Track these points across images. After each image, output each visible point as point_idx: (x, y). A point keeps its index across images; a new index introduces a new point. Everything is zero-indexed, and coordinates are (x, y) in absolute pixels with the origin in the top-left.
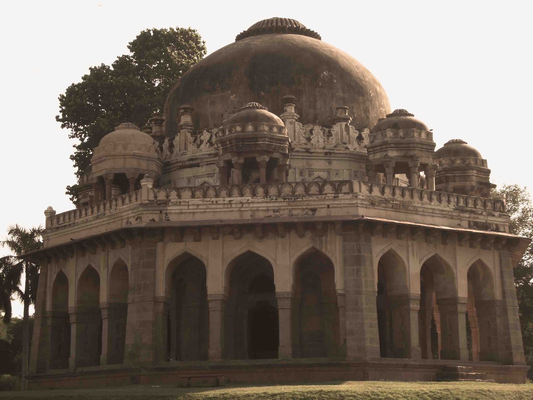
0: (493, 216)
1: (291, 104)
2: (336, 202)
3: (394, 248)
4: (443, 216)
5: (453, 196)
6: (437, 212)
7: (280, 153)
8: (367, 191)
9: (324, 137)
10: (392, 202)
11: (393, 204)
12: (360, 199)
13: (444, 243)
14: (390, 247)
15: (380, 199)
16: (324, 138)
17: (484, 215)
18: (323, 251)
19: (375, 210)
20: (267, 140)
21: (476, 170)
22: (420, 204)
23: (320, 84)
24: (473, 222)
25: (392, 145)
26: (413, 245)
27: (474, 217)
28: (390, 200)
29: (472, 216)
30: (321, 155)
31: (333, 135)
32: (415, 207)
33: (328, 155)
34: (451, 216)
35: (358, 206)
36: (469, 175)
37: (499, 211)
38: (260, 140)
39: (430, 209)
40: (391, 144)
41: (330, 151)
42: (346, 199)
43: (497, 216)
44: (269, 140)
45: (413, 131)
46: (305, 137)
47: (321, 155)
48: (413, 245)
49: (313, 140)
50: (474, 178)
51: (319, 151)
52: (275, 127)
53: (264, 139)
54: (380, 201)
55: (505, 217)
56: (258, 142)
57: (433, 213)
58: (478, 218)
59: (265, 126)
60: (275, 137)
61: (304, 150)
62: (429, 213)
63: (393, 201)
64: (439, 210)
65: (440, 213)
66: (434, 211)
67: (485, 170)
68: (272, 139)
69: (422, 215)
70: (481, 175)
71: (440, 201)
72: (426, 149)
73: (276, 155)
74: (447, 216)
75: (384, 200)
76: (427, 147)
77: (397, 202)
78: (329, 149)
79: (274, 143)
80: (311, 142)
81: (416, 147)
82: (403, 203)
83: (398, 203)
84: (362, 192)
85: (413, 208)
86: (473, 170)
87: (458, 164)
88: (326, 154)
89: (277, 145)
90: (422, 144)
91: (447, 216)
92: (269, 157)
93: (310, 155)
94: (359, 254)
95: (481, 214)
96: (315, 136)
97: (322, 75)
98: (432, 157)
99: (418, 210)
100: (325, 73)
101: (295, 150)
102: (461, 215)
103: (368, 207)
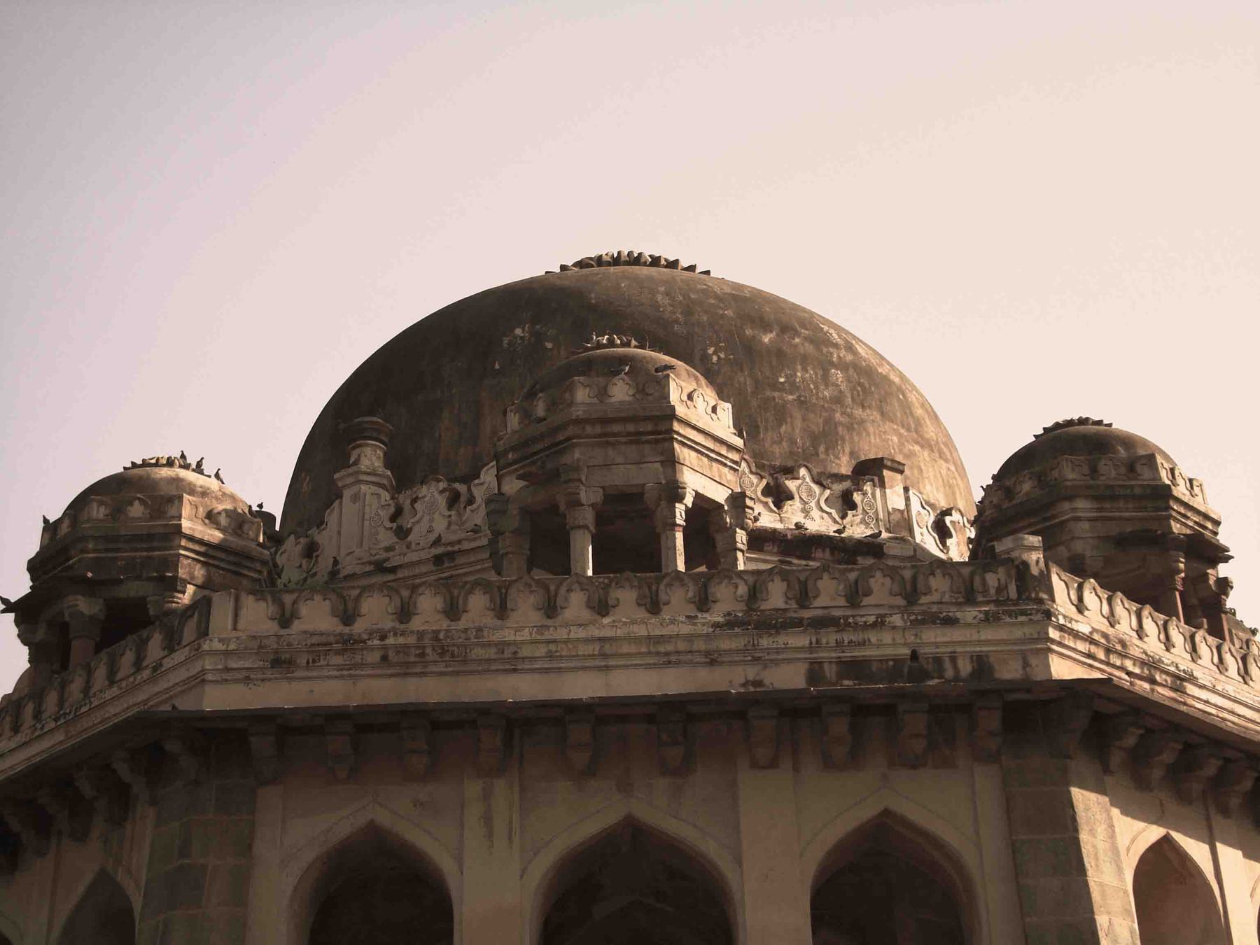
0: (950, 622)
1: (358, 442)
2: (163, 685)
3: (383, 818)
4: (666, 659)
5: (731, 578)
6: (625, 649)
7: (150, 579)
8: (272, 619)
9: (449, 513)
10: (377, 642)
11: (385, 648)
12: (213, 653)
13: (681, 771)
14: (361, 820)
15: (315, 640)
16: (450, 516)
17: (894, 628)
18: (119, 879)
19: (294, 684)
20: (90, 546)
21: (1087, 497)
22: (527, 630)
23: (497, 367)
24: (840, 662)
25: (510, 456)
26: (487, 796)
27: (839, 644)
28: (365, 637)
29: (829, 637)
30: (424, 569)
31: (479, 500)
32: (502, 646)
33: (446, 565)
34: (707, 653)
35: (203, 681)
36: (1068, 520)
37: (997, 602)
38: (73, 552)
39: (586, 641)
40: (506, 452)
41: (449, 548)
42: (181, 664)
43: (969, 620)
44: (100, 547)
45: (571, 389)
46: (392, 528)
47: (424, 569)
48: (487, 796)
49: (416, 529)
50: (1086, 526)
51: (412, 557)
52: (137, 502)
53: (80, 546)
54: (313, 645)
55: (1021, 618)
56: (68, 560)
57: (604, 655)
58: (863, 644)
59: (95, 505)
60: (123, 532)
61: (368, 568)
62: (585, 657)
63: (383, 638)
64: (637, 640)
65: (644, 650)
66: (608, 648)
67: (1137, 491)
68: (111, 540)
69: (546, 671)
70: (1119, 510)
71: (654, 606)
72: (629, 434)
73: (132, 589)
74: (681, 657)
75: (332, 639)
76: (631, 428)
77: (401, 640)
78: (446, 545)
79: (127, 551)
80: (409, 538)
81: (579, 437)
82: (437, 639)
83: (411, 640)
84: (241, 625)
85: (493, 650)
86: (1070, 498)
87: (1027, 494)
88: (438, 560)
89: (135, 558)
90: (605, 421)
91: (681, 657)
92: (101, 601)
93: (391, 577)
94: (186, 861)
95: (879, 624)
96: (421, 518)
97: (506, 341)
98: (662, 458)
99: (520, 655)
100: (518, 331)
101: (341, 575)
102: (765, 642)
103: (252, 676)
